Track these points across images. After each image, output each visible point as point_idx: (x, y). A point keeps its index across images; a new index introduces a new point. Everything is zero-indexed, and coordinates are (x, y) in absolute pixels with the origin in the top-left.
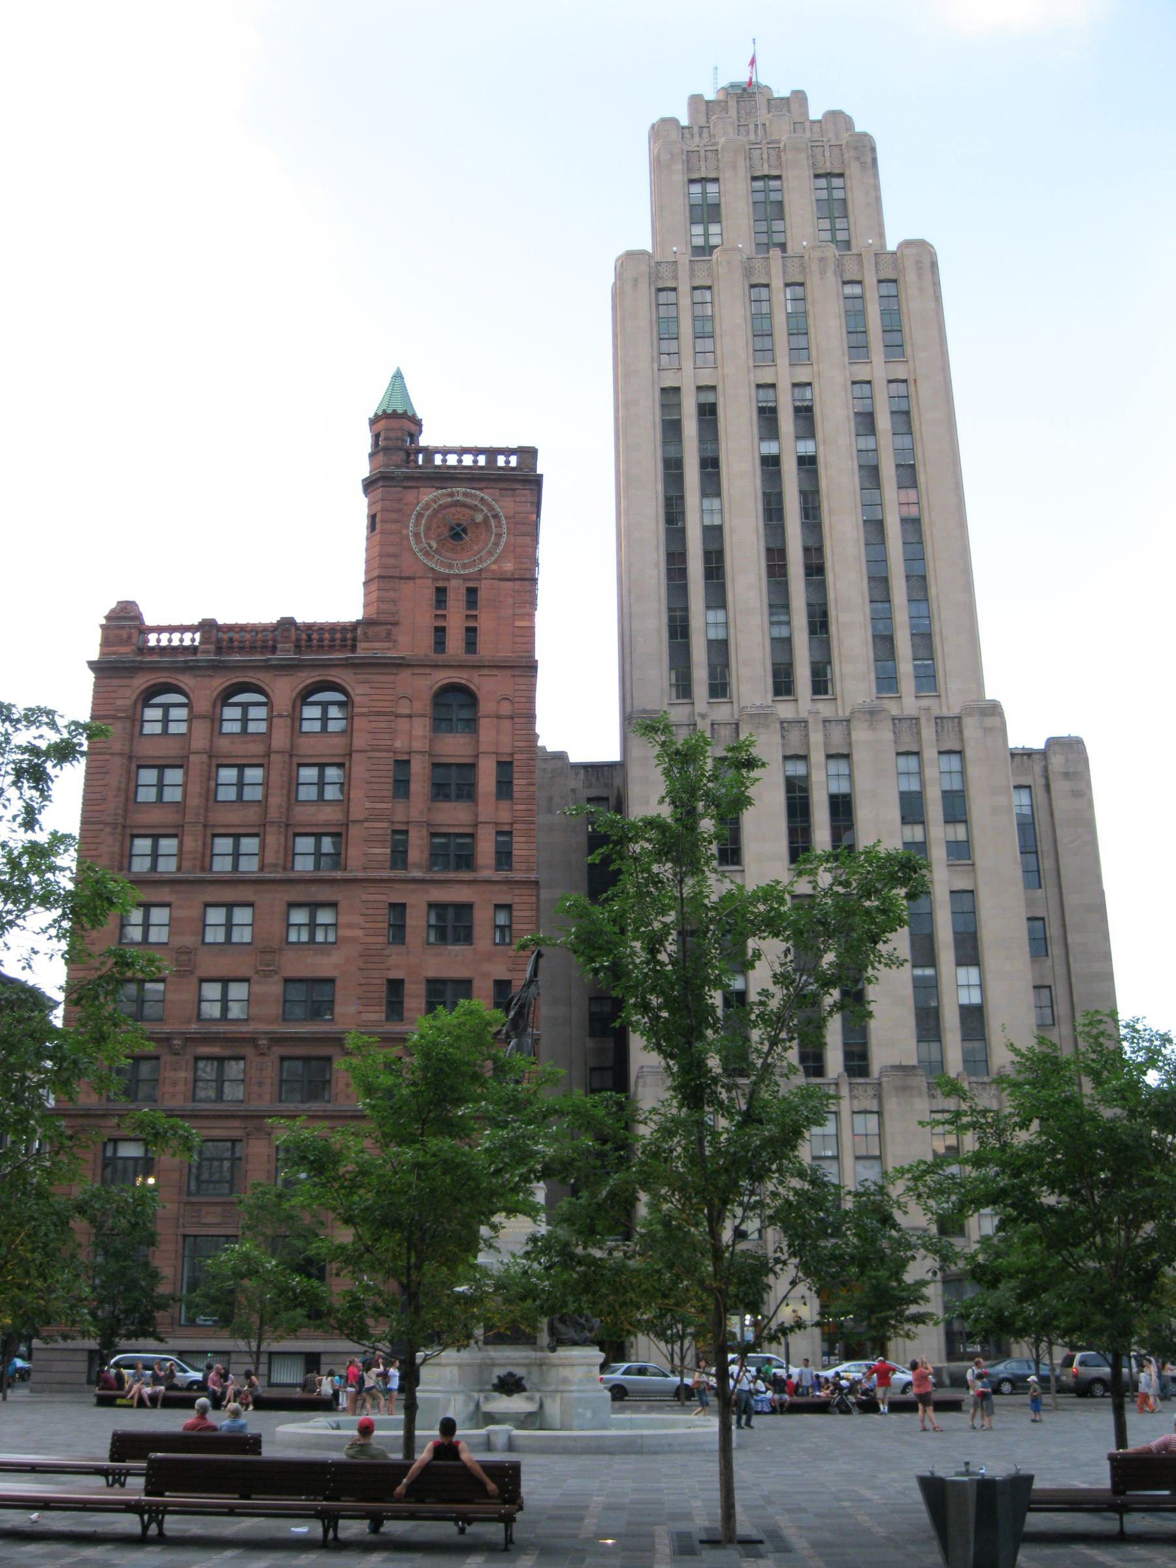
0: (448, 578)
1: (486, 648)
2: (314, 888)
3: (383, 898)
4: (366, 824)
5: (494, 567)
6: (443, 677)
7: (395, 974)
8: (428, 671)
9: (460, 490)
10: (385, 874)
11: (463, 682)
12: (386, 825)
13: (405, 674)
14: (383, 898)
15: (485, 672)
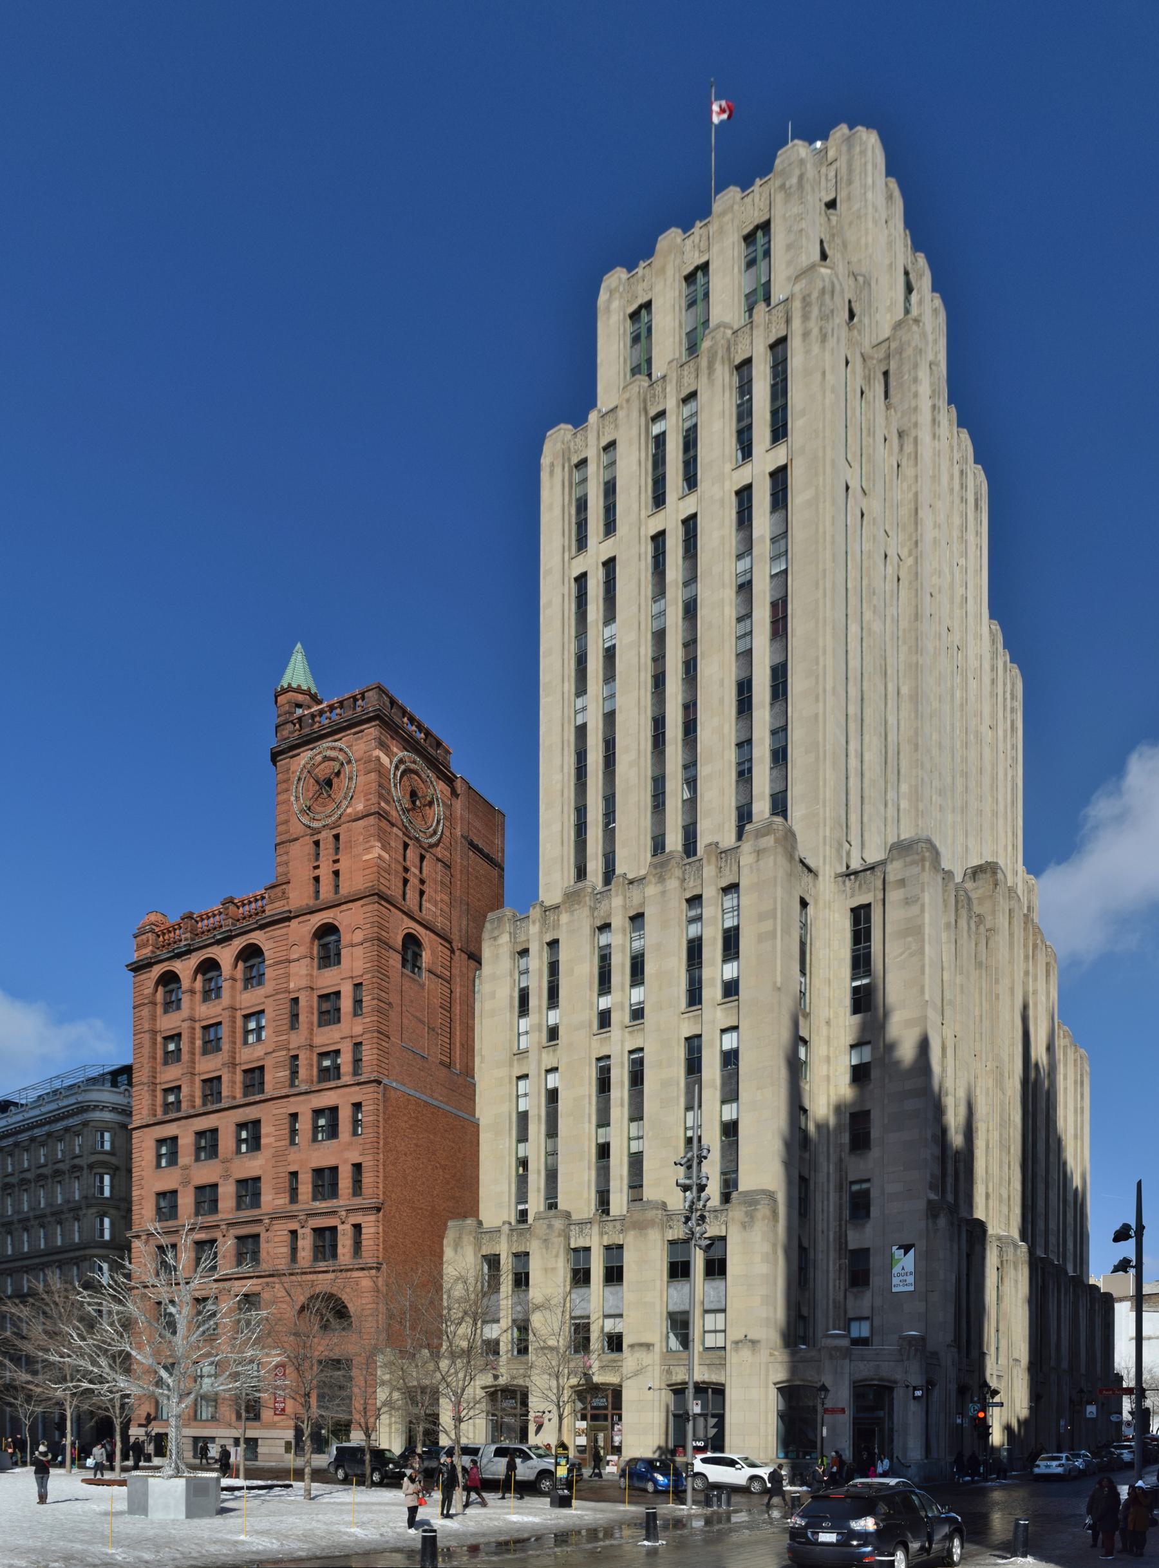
0: (317, 831)
1: (344, 890)
2: (247, 1109)
3: (284, 1110)
4: (274, 1055)
5: (349, 810)
6: (317, 920)
7: (293, 1169)
8: (308, 917)
9: (326, 744)
10: (283, 1092)
11: (330, 921)
12: (284, 1053)
13: (294, 923)
14: (284, 1110)
15: (344, 907)
